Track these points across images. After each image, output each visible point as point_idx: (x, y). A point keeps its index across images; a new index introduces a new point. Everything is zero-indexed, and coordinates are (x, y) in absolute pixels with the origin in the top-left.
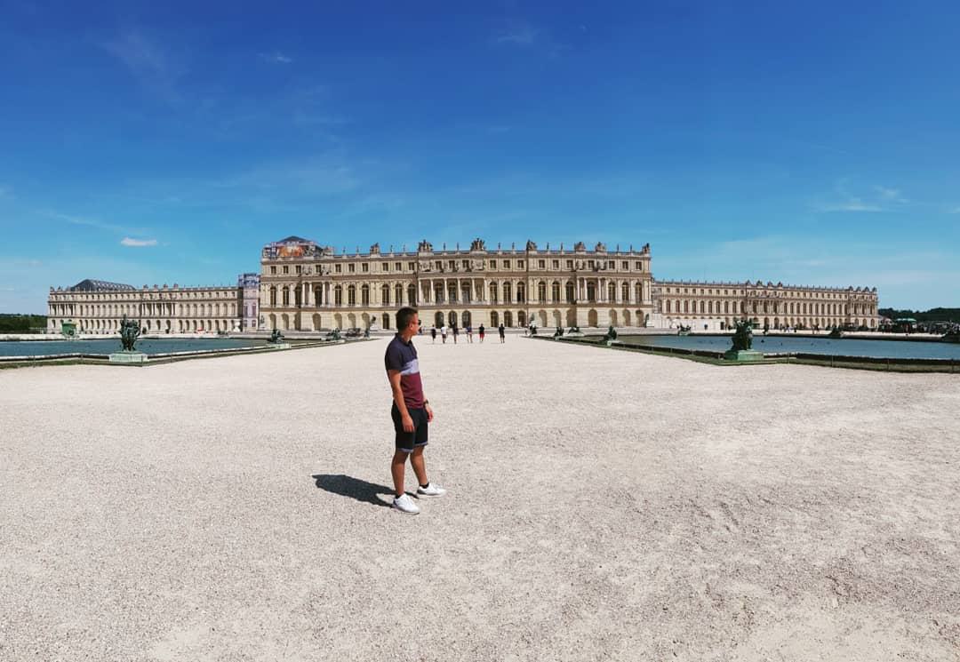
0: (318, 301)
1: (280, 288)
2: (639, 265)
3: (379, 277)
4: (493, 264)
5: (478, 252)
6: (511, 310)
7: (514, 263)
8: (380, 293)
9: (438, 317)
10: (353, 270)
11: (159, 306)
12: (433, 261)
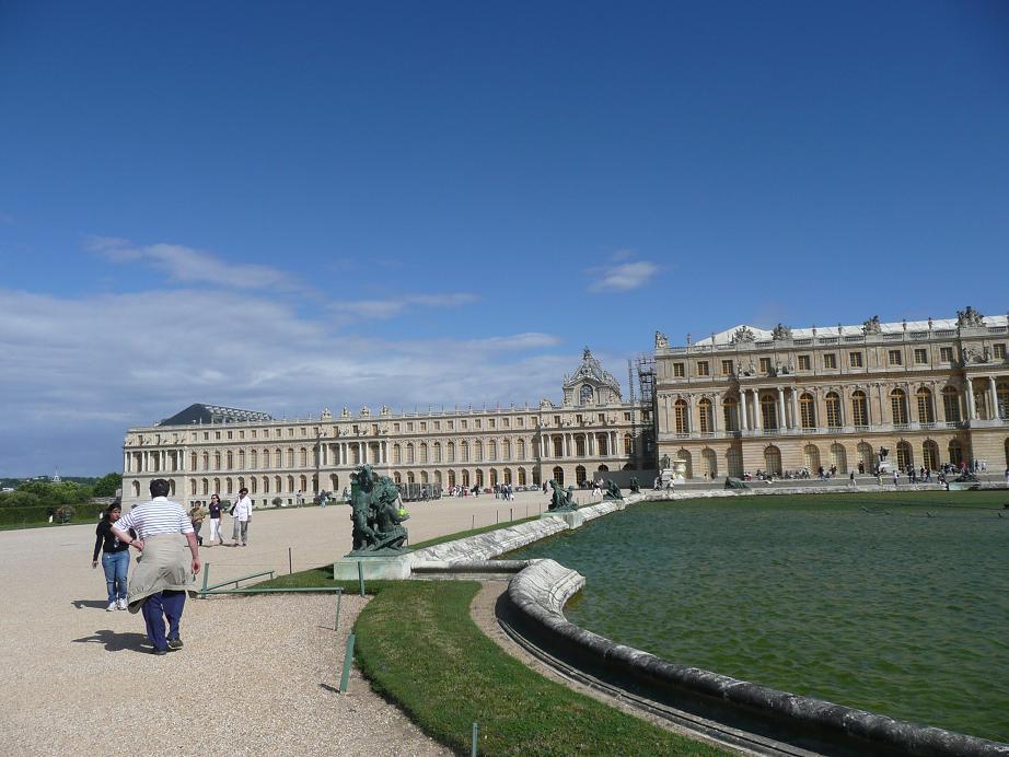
0: (770, 422)
1: (694, 402)
3: (887, 375)
8: (888, 406)
10: (834, 366)
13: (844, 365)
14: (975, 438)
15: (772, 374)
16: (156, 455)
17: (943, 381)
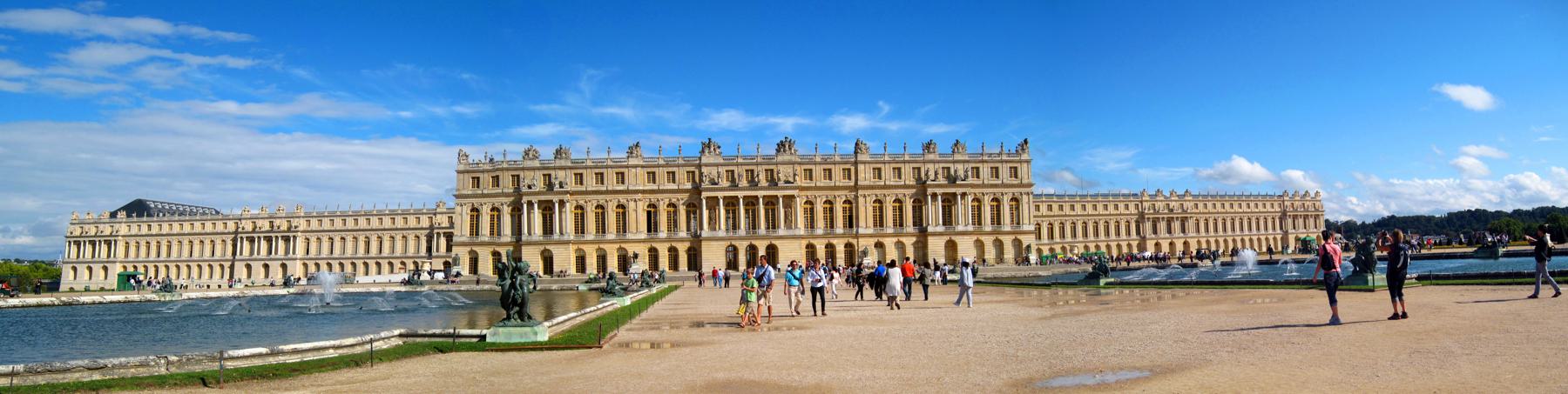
0: (548, 229)
2: (1014, 172)
3: (644, 192)
4: (809, 174)
6: (835, 241)
7: (837, 172)
9: (733, 251)
11: (269, 240)
12: (722, 170)
14: (704, 245)
15: (550, 186)
16: (93, 243)
17: (686, 196)
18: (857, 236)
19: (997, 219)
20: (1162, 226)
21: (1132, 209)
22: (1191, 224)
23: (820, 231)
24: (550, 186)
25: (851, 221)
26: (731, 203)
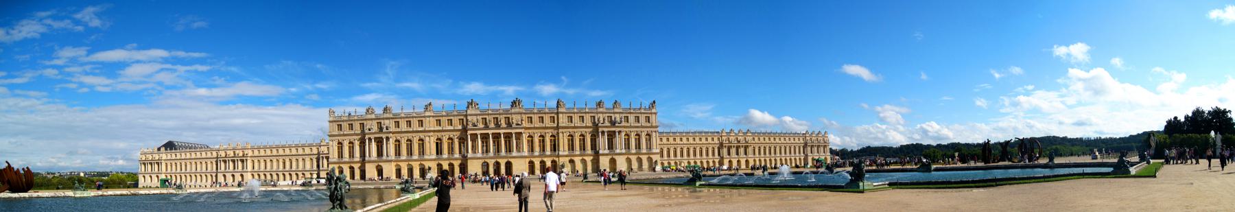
0: (380, 154)
2: (648, 119)
5: (517, 110)
7: (547, 118)
12: (480, 118)
13: (415, 126)
15: (381, 129)
17: (458, 134)
18: (558, 156)
19: (638, 146)
20: (733, 151)
21: (716, 141)
22: (750, 150)
23: (537, 153)
24: (381, 129)
25: (555, 147)
26: (485, 137)
